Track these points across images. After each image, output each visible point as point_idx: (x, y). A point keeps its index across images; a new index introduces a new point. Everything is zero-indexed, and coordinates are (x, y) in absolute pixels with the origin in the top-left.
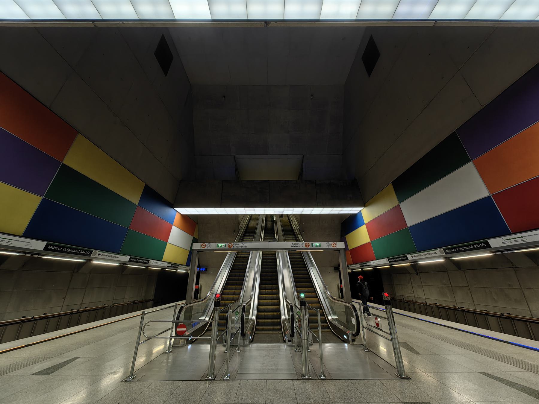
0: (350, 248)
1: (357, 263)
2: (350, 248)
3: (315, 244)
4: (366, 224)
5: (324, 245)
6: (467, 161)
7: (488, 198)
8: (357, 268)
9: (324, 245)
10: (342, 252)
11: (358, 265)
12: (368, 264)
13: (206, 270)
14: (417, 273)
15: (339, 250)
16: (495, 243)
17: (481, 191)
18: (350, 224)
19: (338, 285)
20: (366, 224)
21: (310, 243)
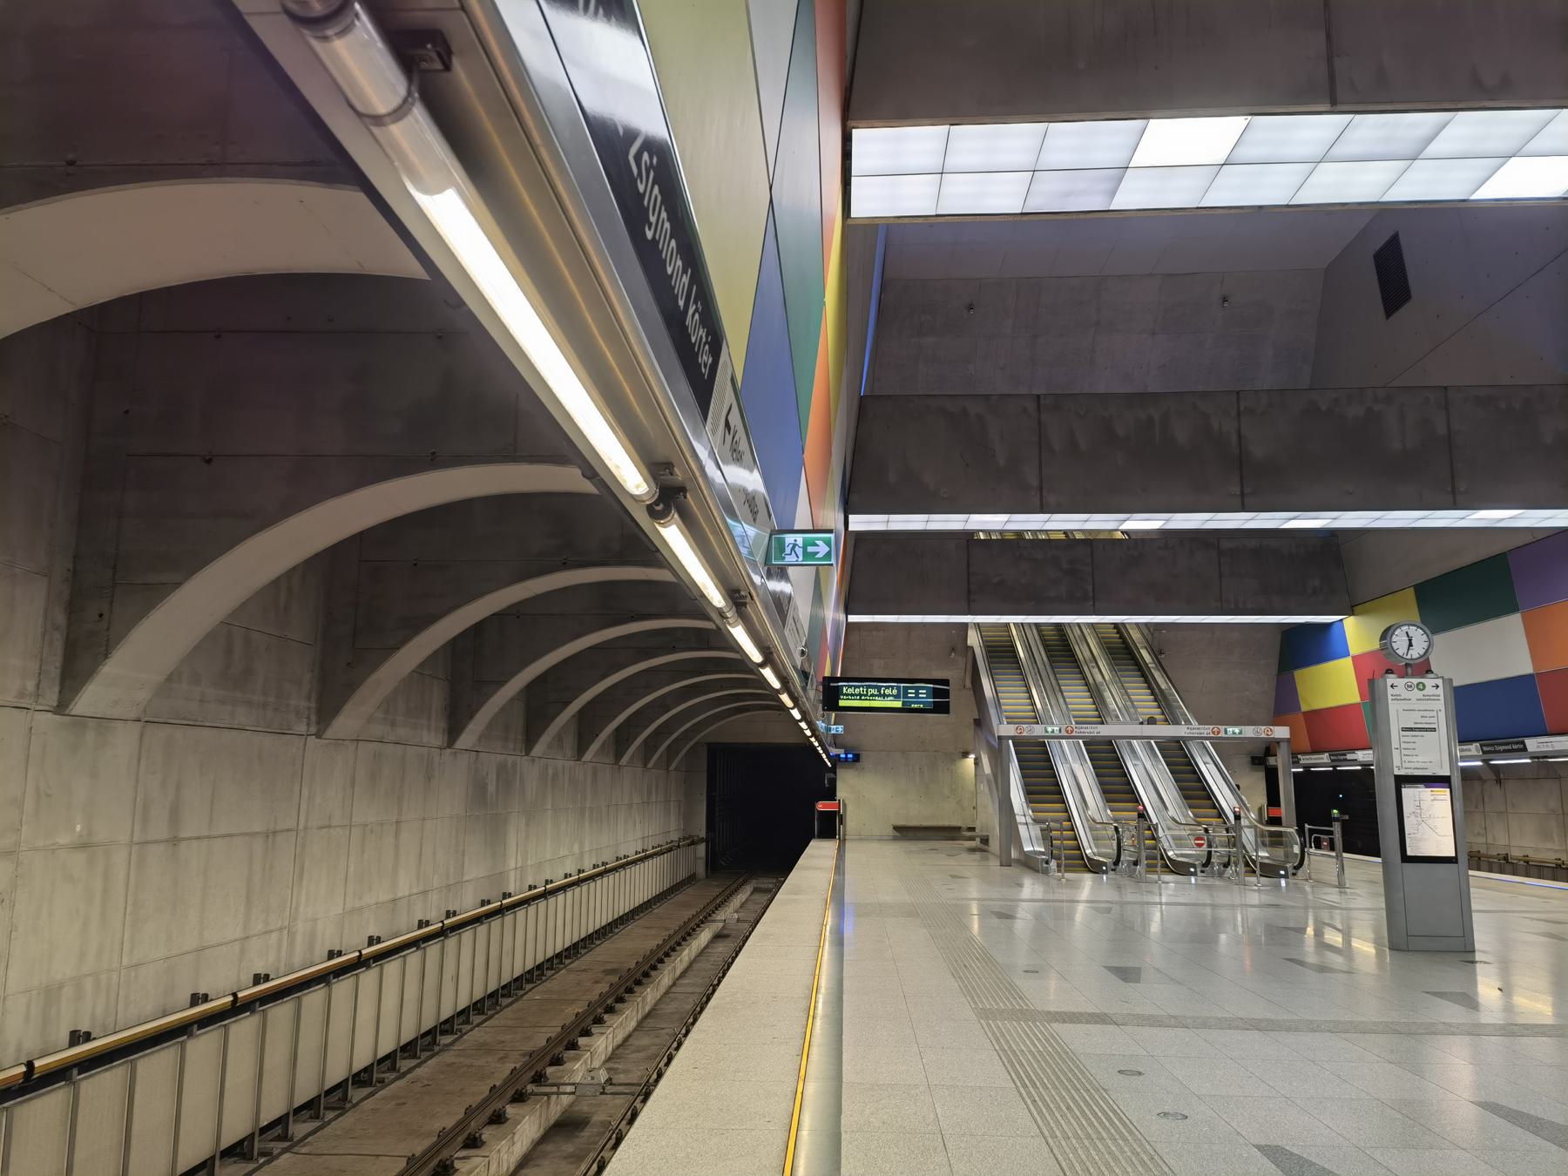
0: (1304, 708)
1: (1323, 752)
2: (1304, 708)
3: (1230, 730)
4: (1355, 659)
5: (1249, 731)
6: (1512, 609)
7: (1530, 677)
8: (1321, 762)
9: (1249, 731)
10: (1284, 746)
11: (1325, 758)
12: (1349, 757)
13: (857, 758)
14: (1499, 781)
15: (1278, 742)
16: (1532, 744)
17: (1522, 665)
18: (1307, 647)
19: (1260, 810)
20: (1355, 659)
21: (1222, 728)
